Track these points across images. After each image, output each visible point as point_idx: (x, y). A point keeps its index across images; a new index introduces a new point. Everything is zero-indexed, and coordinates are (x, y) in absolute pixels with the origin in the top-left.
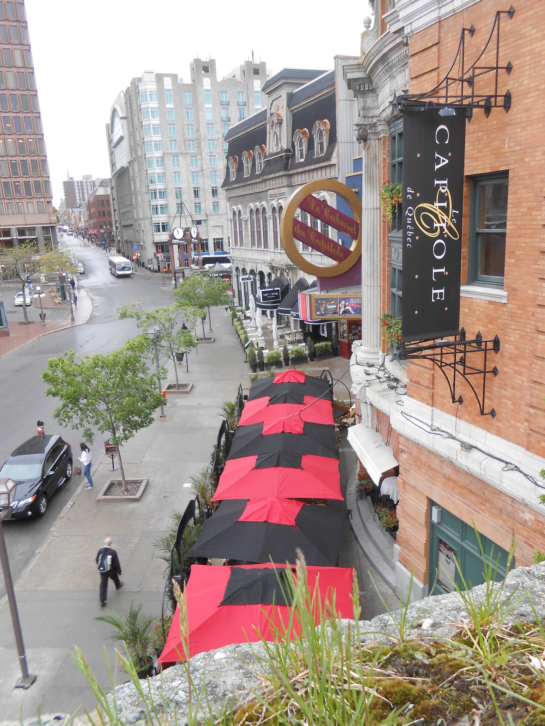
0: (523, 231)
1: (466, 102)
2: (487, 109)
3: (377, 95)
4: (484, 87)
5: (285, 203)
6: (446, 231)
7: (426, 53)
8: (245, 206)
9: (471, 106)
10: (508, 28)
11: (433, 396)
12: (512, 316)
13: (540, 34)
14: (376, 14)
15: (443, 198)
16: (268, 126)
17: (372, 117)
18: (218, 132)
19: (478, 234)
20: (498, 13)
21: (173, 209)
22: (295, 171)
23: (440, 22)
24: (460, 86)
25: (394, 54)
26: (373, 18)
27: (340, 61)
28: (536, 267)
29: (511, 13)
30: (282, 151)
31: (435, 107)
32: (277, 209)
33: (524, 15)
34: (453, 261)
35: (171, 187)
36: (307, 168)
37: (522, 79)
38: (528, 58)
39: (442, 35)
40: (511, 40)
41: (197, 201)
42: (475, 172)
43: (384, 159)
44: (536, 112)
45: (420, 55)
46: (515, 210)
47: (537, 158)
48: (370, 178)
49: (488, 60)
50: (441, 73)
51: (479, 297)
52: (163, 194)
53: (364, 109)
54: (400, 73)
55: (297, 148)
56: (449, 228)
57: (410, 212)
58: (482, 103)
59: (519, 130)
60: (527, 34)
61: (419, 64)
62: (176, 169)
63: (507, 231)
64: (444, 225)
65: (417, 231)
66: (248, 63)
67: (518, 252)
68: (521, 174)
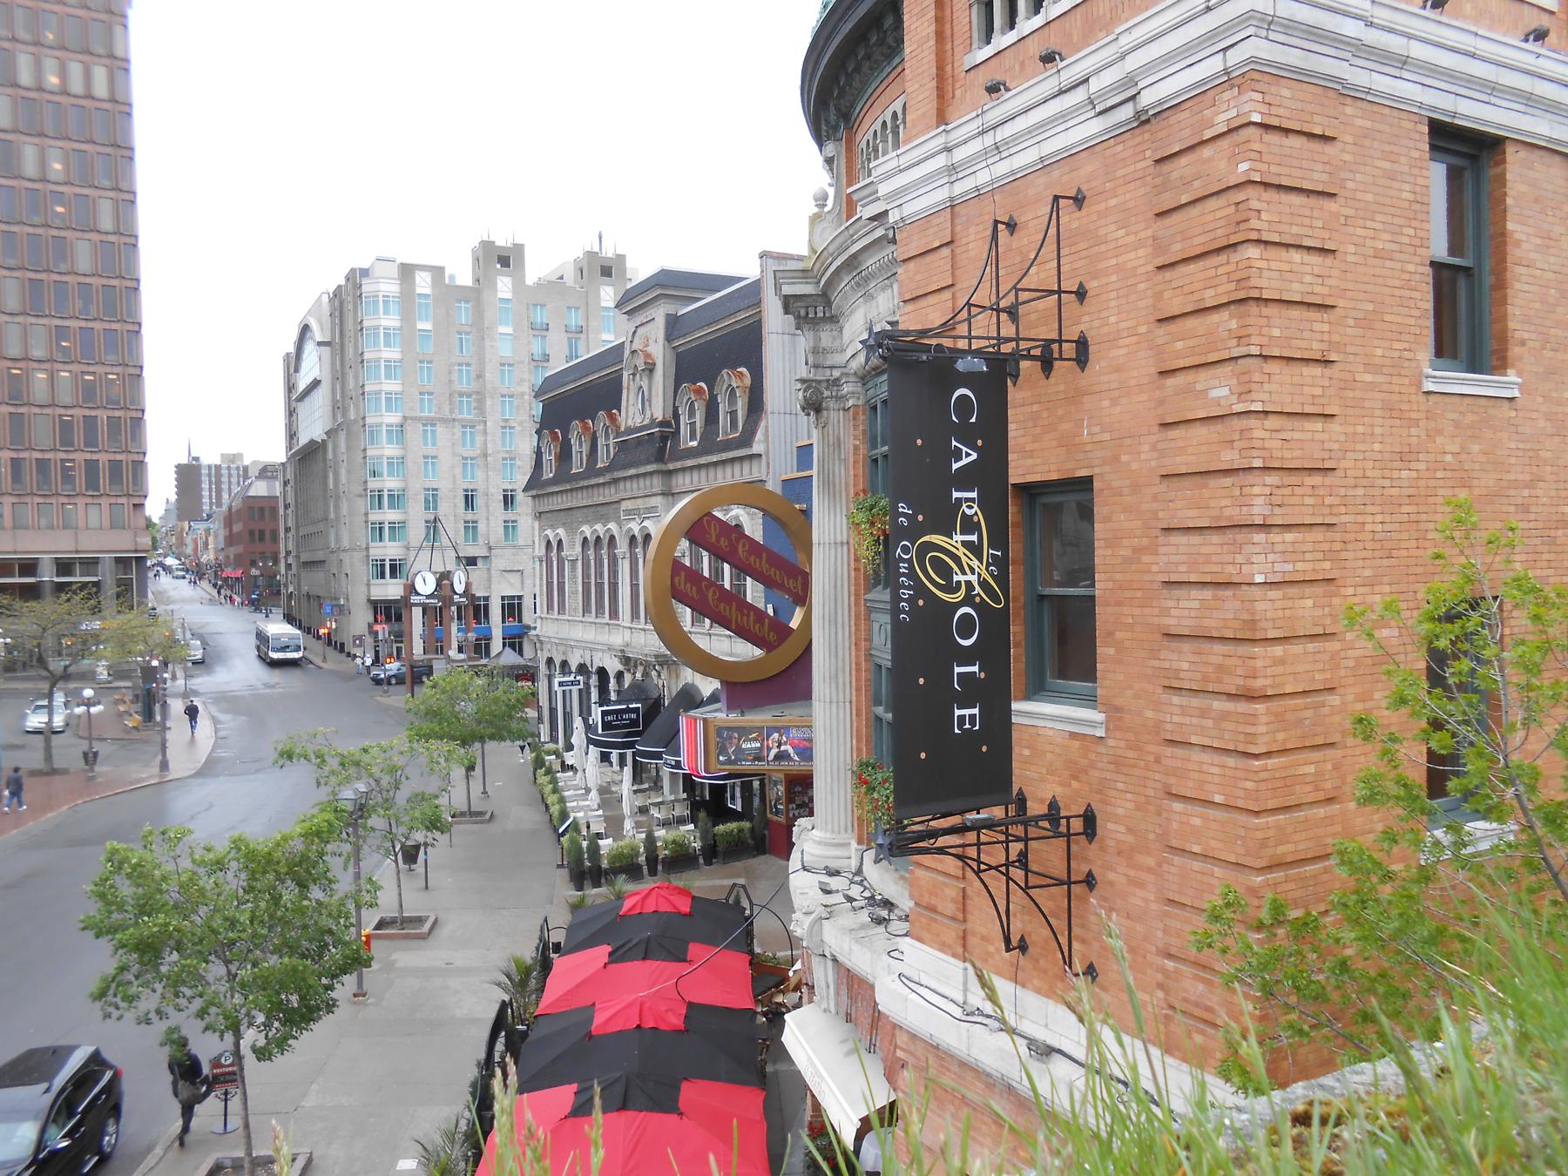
0: (1128, 594)
1: (1006, 348)
2: (1047, 364)
3: (841, 328)
4: (1038, 322)
5: (655, 528)
6: (978, 590)
7: (929, 258)
8: (572, 529)
9: (1016, 356)
10: (1075, 224)
11: (964, 938)
12: (1117, 763)
13: (1131, 238)
14: (837, 184)
15: (969, 526)
16: (625, 375)
17: (832, 367)
18: (522, 380)
19: (1042, 597)
20: (1056, 198)
21: (417, 532)
22: (678, 465)
23: (952, 206)
24: (994, 319)
25: (870, 257)
26: (831, 192)
27: (770, 261)
28: (1156, 663)
29: (1079, 200)
30: (653, 423)
31: (948, 354)
32: (640, 539)
33: (1102, 206)
34: (993, 650)
35: (417, 487)
36: (703, 460)
37: (1105, 314)
38: (1114, 278)
39: (958, 229)
40: (1083, 245)
41: (469, 517)
42: (1029, 479)
43: (856, 448)
44: (1135, 373)
45: (919, 260)
46: (1109, 552)
47: (1143, 457)
48: (828, 483)
49: (1041, 276)
50: (959, 295)
51: (1050, 724)
52: (396, 500)
53: (815, 351)
54: (883, 289)
55: (684, 419)
56: (984, 584)
57: (906, 550)
58: (1036, 352)
59: (1106, 403)
60: (1109, 237)
61: (918, 277)
62: (430, 450)
63: (1097, 593)
64: (974, 579)
65: (920, 590)
66: (591, 255)
67: (1118, 635)
68: (1116, 484)
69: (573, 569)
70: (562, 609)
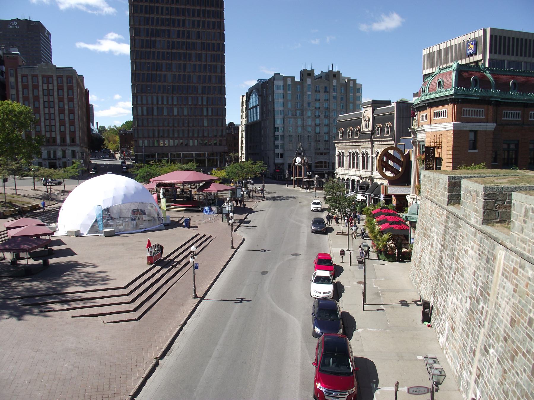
8: (346, 150)
69: (346, 158)
70: (343, 166)
